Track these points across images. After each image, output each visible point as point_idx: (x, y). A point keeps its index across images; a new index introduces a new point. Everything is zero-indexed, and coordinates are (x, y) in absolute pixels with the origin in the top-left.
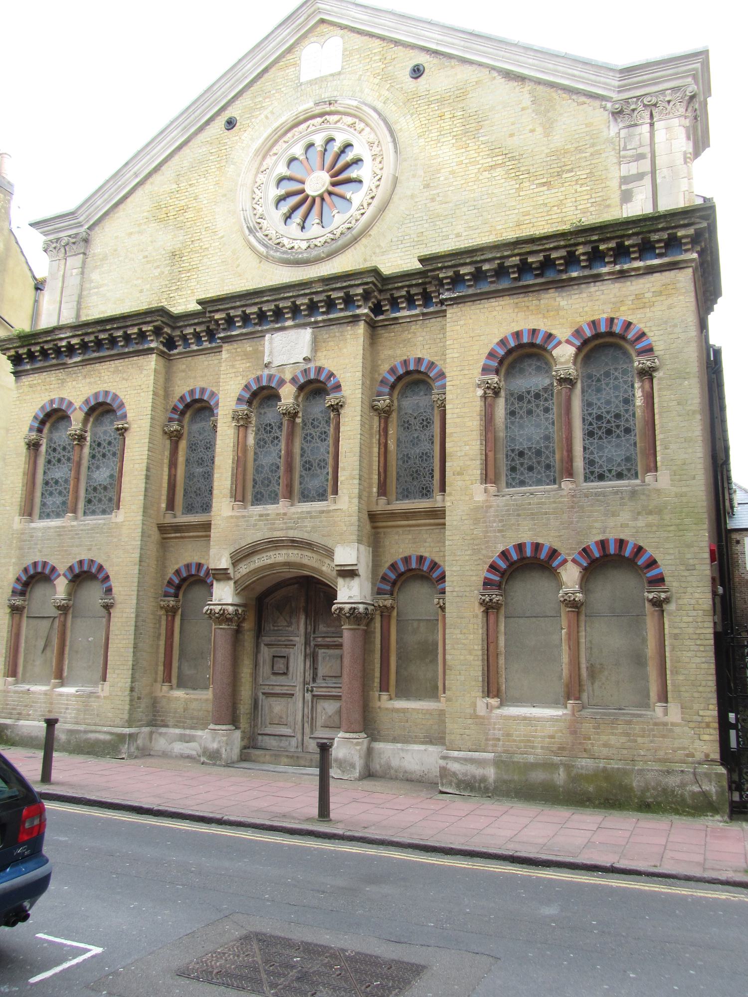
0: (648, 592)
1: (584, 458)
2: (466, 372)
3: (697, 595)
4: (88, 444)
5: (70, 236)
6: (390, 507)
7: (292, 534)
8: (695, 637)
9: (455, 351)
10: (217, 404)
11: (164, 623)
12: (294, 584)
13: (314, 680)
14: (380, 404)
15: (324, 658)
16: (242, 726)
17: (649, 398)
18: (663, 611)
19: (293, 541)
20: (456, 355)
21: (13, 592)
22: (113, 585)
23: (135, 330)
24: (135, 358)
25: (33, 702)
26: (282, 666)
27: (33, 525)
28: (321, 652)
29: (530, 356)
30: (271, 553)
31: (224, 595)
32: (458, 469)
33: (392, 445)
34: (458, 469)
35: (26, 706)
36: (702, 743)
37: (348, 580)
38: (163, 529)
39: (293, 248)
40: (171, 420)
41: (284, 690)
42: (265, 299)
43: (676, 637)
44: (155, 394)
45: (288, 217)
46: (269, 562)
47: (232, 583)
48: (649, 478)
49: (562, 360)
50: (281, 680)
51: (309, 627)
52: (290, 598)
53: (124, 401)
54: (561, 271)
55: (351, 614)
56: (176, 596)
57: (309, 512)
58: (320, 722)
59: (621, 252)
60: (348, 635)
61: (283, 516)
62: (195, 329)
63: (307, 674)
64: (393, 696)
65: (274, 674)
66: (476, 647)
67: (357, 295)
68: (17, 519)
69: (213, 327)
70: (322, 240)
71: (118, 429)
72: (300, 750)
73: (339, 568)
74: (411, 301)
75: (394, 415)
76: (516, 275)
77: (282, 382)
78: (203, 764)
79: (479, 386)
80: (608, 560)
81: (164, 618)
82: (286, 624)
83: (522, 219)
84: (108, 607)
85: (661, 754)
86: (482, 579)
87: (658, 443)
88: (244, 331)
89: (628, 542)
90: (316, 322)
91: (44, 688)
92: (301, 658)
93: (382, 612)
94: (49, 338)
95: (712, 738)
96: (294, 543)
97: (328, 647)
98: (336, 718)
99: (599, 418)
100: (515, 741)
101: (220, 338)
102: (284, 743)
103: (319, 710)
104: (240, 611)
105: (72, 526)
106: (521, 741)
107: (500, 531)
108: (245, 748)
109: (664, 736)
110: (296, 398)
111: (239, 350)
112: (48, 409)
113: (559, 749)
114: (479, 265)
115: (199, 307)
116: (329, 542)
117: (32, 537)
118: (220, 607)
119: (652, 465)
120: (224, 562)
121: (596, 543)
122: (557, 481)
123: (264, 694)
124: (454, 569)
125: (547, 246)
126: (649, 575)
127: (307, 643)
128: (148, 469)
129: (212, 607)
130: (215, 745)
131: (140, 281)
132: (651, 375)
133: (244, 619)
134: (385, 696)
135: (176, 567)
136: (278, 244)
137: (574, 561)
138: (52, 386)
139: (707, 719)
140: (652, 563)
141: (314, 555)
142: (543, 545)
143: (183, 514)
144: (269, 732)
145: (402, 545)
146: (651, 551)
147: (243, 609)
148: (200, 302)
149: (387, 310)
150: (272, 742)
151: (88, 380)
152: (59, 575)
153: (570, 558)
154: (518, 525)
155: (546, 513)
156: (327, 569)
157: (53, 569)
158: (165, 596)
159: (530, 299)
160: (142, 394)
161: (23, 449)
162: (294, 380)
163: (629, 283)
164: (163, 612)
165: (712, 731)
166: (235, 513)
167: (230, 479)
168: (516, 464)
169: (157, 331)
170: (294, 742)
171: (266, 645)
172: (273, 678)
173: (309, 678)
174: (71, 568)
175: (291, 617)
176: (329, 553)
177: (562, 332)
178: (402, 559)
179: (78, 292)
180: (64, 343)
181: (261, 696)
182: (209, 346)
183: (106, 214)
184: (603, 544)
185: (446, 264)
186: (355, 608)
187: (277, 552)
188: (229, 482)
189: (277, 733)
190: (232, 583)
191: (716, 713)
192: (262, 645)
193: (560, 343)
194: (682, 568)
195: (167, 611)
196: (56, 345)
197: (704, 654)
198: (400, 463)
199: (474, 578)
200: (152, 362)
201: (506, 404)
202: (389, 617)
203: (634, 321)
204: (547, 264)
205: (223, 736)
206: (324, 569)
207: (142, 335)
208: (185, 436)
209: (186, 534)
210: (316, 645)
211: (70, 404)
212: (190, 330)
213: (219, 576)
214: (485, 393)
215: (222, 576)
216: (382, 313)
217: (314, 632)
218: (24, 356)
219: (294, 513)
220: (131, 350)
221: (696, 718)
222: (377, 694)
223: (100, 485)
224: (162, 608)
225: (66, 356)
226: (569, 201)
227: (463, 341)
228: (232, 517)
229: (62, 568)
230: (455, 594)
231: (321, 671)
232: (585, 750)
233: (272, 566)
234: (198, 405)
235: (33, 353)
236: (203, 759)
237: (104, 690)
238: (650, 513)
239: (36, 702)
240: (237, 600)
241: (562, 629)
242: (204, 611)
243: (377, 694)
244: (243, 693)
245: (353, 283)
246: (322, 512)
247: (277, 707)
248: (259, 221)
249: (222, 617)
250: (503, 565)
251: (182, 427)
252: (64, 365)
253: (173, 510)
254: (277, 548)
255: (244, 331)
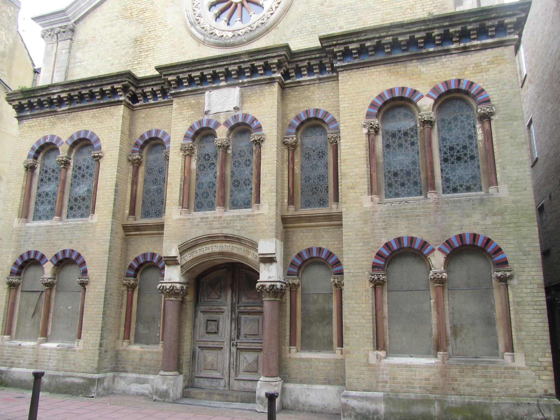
0: (497, 271)
1: (442, 177)
2: (355, 117)
3: (533, 273)
4: (71, 168)
5: (61, 27)
6: (297, 213)
7: (226, 231)
8: (533, 303)
9: (346, 102)
10: (169, 141)
11: (125, 296)
12: (223, 268)
13: (238, 337)
14: (290, 141)
15: (245, 321)
16: (184, 371)
17: (488, 135)
18: (507, 285)
19: (226, 237)
20: (347, 105)
21: (11, 273)
22: (88, 268)
23: (109, 87)
24: (108, 108)
25: (24, 354)
26: (214, 327)
27: (28, 225)
28: (243, 317)
29: (400, 106)
30: (210, 246)
31: (173, 276)
32: (351, 184)
33: (297, 169)
34: (351, 184)
35: (18, 357)
36: (542, 382)
37: (267, 265)
38: (126, 228)
39: (222, 36)
40: (133, 152)
41: (216, 345)
42: (206, 66)
43: (518, 304)
44: (122, 132)
45: (218, 17)
46: (208, 252)
47: (179, 267)
48: (492, 190)
49: (425, 108)
50: (213, 337)
51: (234, 299)
52: (223, 278)
53: (99, 137)
54: (421, 48)
55: (271, 290)
56: (135, 276)
57: (238, 216)
58: (242, 368)
59: (464, 35)
60: (268, 304)
61: (220, 219)
62: (152, 89)
63: (233, 333)
64: (299, 349)
65: (208, 333)
66: (368, 313)
67: (273, 64)
68: (16, 220)
69: (165, 87)
70: (243, 31)
71: (94, 157)
72: (227, 388)
73: (261, 256)
74: (310, 70)
75: (299, 149)
76: (389, 50)
77: (217, 124)
78: (154, 401)
79: (364, 126)
80: (466, 248)
81: (126, 292)
82: (217, 297)
83: (385, 17)
84: (84, 285)
85: (511, 391)
86: (371, 264)
87: (497, 165)
88: (190, 89)
89: (479, 235)
90: (243, 83)
91: (32, 344)
92: (228, 322)
93: (291, 288)
94: (45, 93)
95: (549, 378)
96: (227, 238)
97: (249, 313)
98: (255, 365)
99: (452, 149)
100: (399, 383)
101: (172, 94)
102: (215, 384)
103: (242, 359)
104: (185, 288)
105: (58, 225)
106: (403, 383)
107: (383, 229)
108: (186, 387)
109: (513, 377)
110: (228, 135)
111: (185, 102)
112: (42, 143)
113: (433, 388)
114: (363, 43)
115: (157, 73)
116: (254, 238)
117: (27, 233)
118: (170, 285)
119: (494, 181)
120: (174, 252)
121: (456, 236)
122: (423, 193)
123: (199, 347)
124: (350, 256)
125: (412, 30)
126: (496, 259)
127: (233, 311)
128: (117, 185)
129: (164, 285)
130: (165, 387)
131: (111, 58)
132: (489, 118)
133: (187, 293)
134: (293, 349)
135: (136, 256)
136: (212, 33)
137: (440, 249)
138: (46, 127)
139: (545, 364)
140: (498, 250)
141: (242, 247)
142: (416, 238)
143: (141, 218)
144: (203, 376)
145: (306, 240)
146: (497, 241)
147: (187, 286)
148: (158, 69)
149: (293, 76)
150: (206, 383)
151: (72, 123)
152: (47, 261)
153: (436, 248)
154: (397, 224)
155: (418, 216)
156: (251, 257)
157: (43, 256)
158: (127, 276)
159: (399, 67)
160: (113, 133)
161: (23, 171)
162: (226, 123)
163: (470, 56)
164: (125, 288)
165: (548, 373)
166: (183, 217)
167: (178, 192)
168: (392, 182)
169: (125, 89)
170: (222, 383)
171: (202, 312)
172: (207, 336)
173: (234, 335)
174: (56, 256)
175: (220, 292)
176: (254, 246)
177: (424, 89)
178: (306, 250)
179: (66, 65)
181: (198, 350)
182: (163, 100)
183: (87, 13)
184: (461, 237)
185: (339, 42)
186: (273, 285)
187: (214, 245)
188: (178, 195)
189: (207, 376)
190: (179, 267)
191: (551, 359)
192: (199, 312)
193: (422, 97)
194: (521, 253)
195: (128, 288)
196: (50, 98)
197: (540, 316)
198: (304, 182)
199: (365, 263)
200: (121, 110)
201: (383, 140)
202: (296, 291)
203: (475, 82)
204: (412, 42)
205: (171, 380)
206: (250, 257)
207: (114, 92)
208: (144, 163)
209: (144, 232)
210: (239, 312)
211: (59, 139)
212: (149, 89)
213: (170, 262)
214: (369, 131)
215: (173, 262)
216: (289, 78)
217: (238, 303)
218: (26, 106)
219: (227, 217)
220: (105, 101)
221: (536, 363)
222: (288, 348)
223: (80, 197)
224: (124, 285)
225: (57, 106)
226: (418, 5)
227: (351, 95)
228: (180, 219)
229: (49, 256)
230: (351, 274)
231: (243, 331)
232: (453, 389)
233: (210, 255)
234: (153, 142)
235: (32, 103)
236: (155, 397)
237: (79, 346)
238: (495, 215)
239: (26, 354)
240: (182, 280)
241: (431, 299)
242: (158, 287)
243: (288, 348)
244: (185, 347)
245: (270, 55)
246: (249, 216)
247: (210, 356)
248: (197, 18)
249: (172, 292)
250: (386, 253)
251: (142, 157)
253: (134, 215)
254: (213, 242)
255: (190, 89)
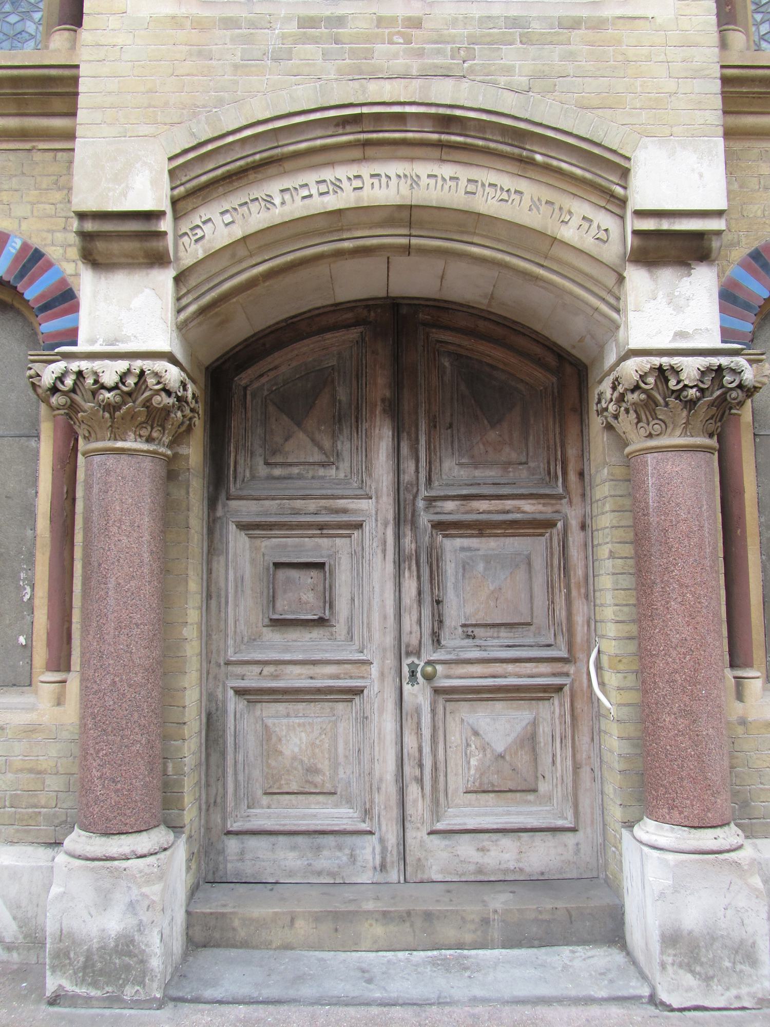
13: (436, 640)
15: (465, 567)
26: (309, 597)
28: (453, 547)
41: (324, 677)
51: (409, 466)
58: (456, 781)
63: (409, 622)
65: (279, 623)
72: (394, 875)
82: (317, 457)
92: (381, 569)
97: (481, 528)
98: (523, 760)
102: (330, 858)
103: (456, 736)
127: (403, 517)
144: (268, 825)
150: (287, 859)
170: (368, 850)
171: (243, 527)
172: (274, 637)
175: (334, 437)
192: (232, 528)
210: (439, 526)
231: (456, 611)
247: (298, 734)
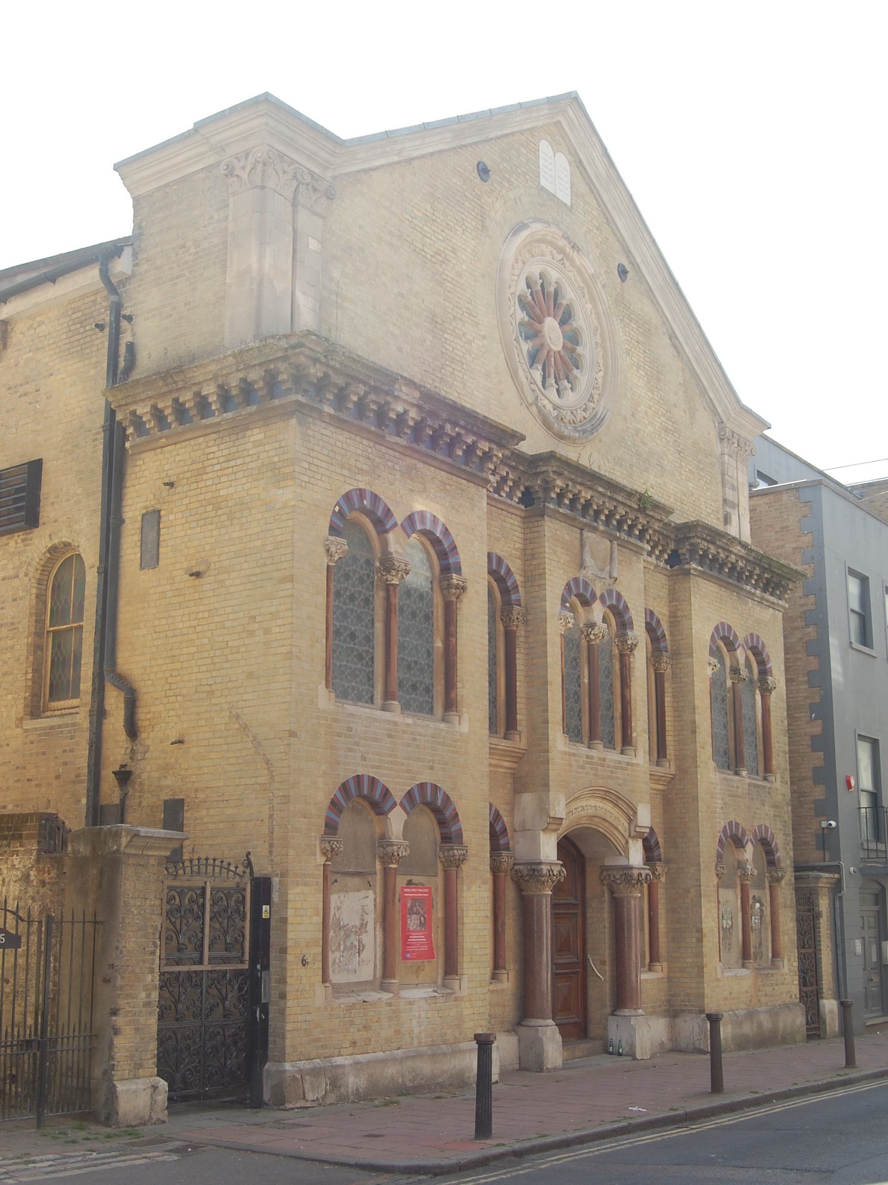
105: (406, 724)
117: (350, 729)
152: (395, 805)
157: (386, 793)
180: (400, 409)
196: (387, 403)
252: (379, 439)
